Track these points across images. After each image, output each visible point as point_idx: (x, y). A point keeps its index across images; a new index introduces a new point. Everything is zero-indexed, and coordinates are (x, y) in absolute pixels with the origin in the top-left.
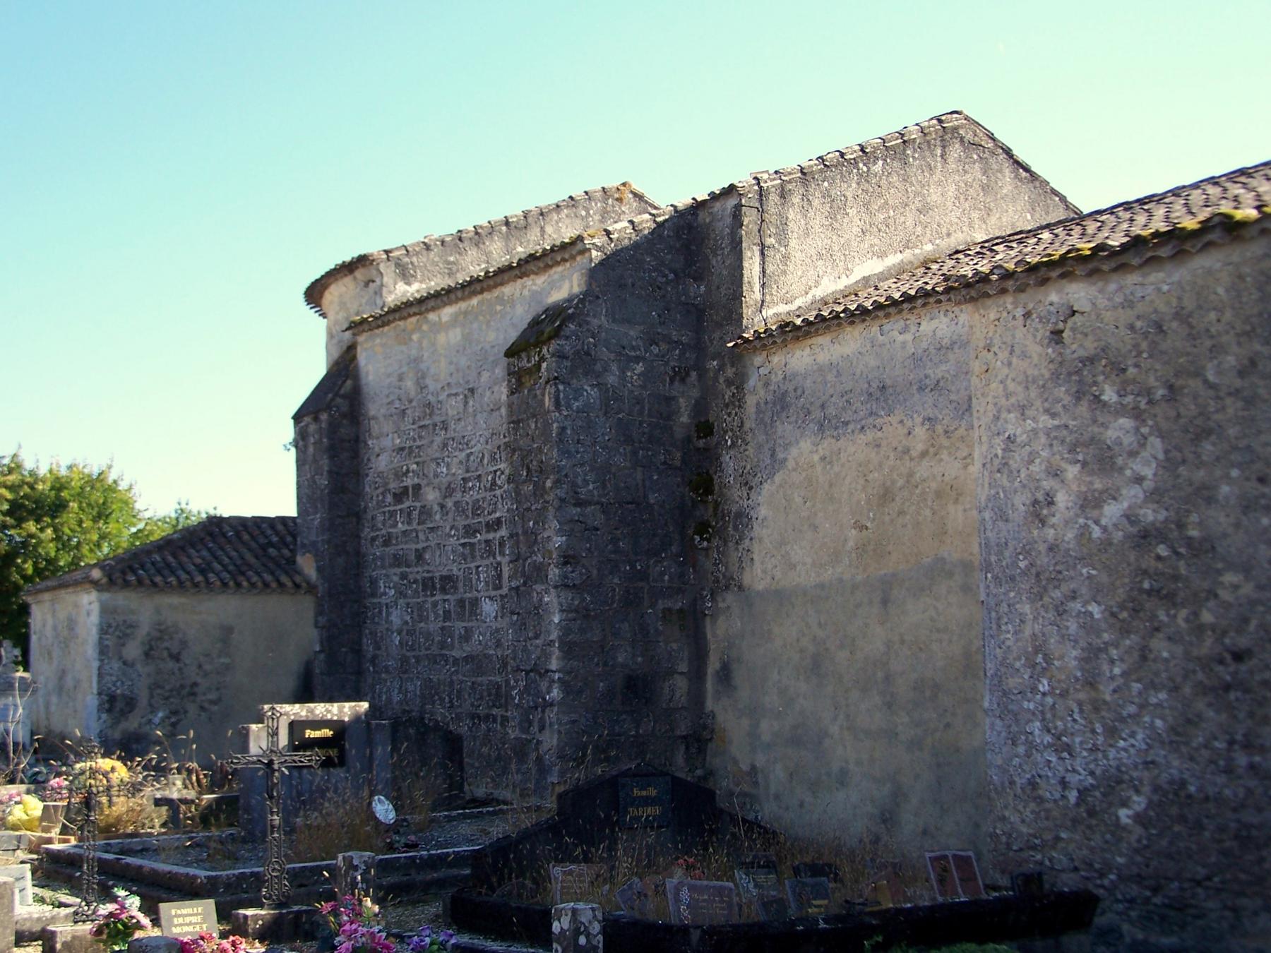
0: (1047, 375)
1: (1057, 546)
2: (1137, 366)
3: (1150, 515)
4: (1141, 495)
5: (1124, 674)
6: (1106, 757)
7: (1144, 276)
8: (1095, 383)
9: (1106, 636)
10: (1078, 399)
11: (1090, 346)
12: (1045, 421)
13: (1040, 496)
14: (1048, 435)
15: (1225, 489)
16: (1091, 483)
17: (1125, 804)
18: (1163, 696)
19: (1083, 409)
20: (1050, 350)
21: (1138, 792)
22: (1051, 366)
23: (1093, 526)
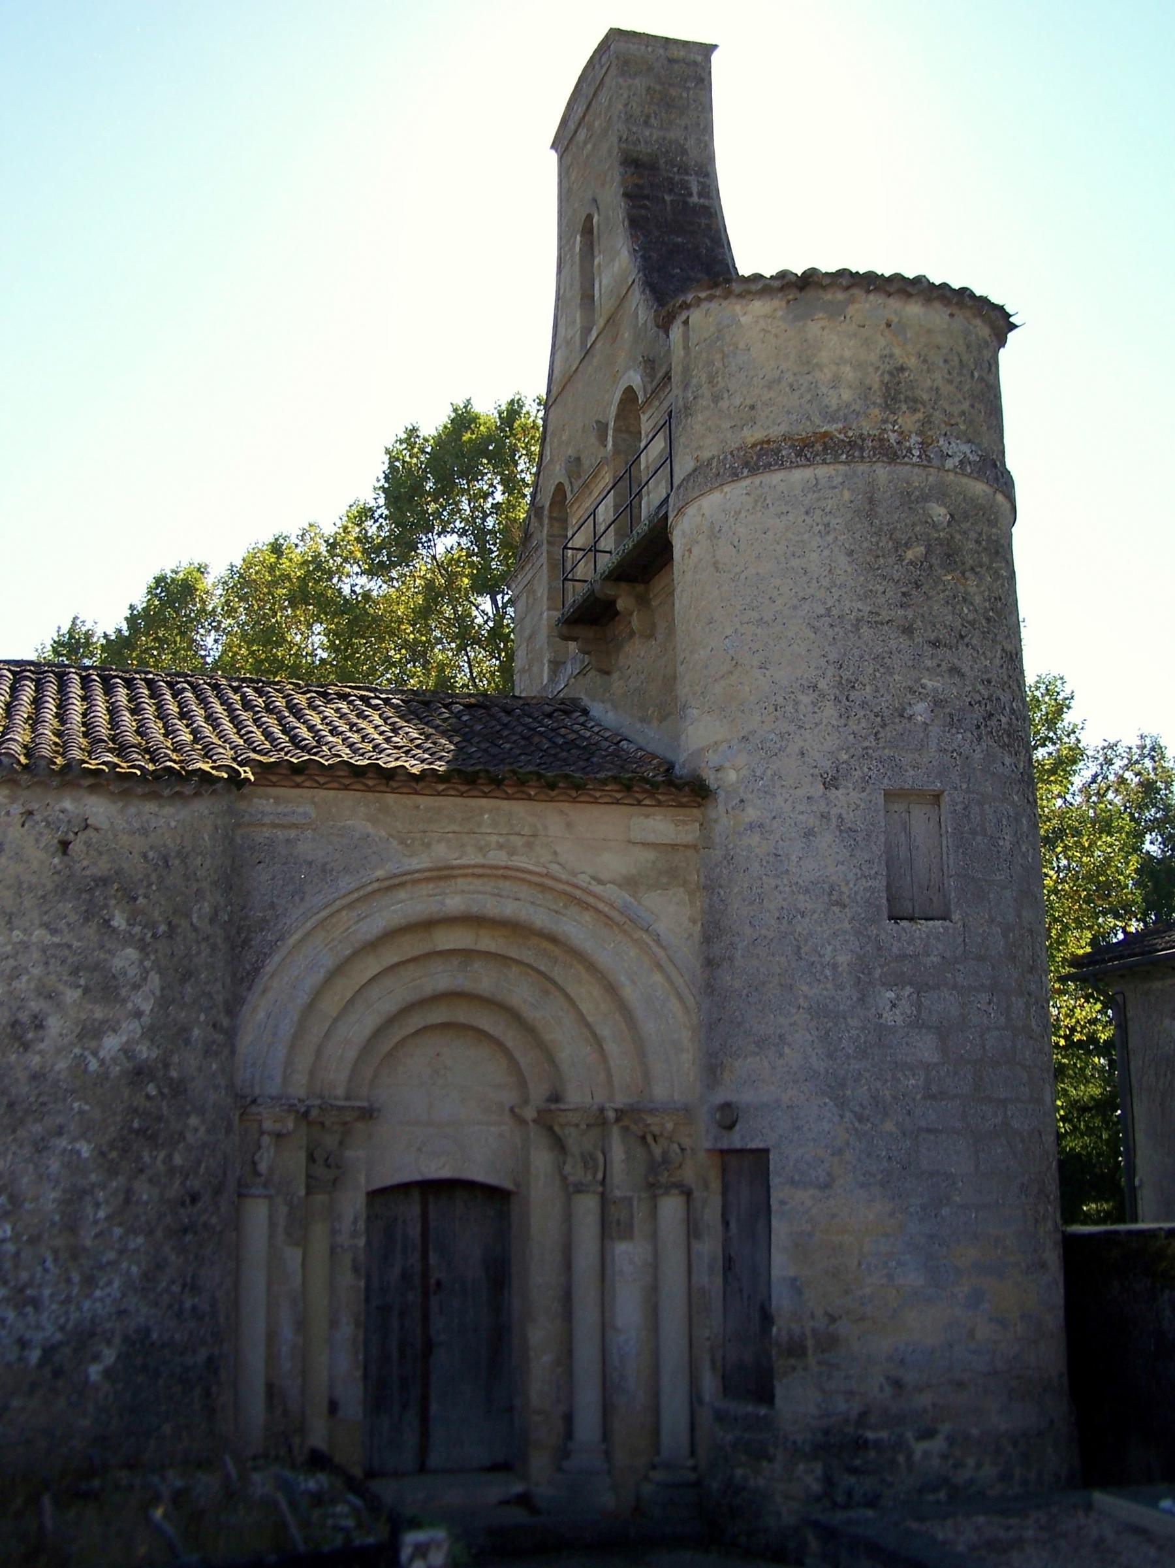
0: (50, 886)
1: (44, 1075)
2: (146, 896)
3: (144, 1052)
4: (139, 1031)
5: (108, 1218)
6: (80, 1309)
7: (161, 806)
8: (106, 906)
9: (93, 1177)
10: (87, 920)
11: (103, 867)
12: (39, 934)
13: (24, 1017)
14: (44, 951)
15: (196, 1032)
16: (91, 1011)
17: (96, 1358)
18: (140, 1240)
19: (90, 931)
20: (56, 860)
21: (109, 1343)
22: (56, 877)
23: (90, 1057)
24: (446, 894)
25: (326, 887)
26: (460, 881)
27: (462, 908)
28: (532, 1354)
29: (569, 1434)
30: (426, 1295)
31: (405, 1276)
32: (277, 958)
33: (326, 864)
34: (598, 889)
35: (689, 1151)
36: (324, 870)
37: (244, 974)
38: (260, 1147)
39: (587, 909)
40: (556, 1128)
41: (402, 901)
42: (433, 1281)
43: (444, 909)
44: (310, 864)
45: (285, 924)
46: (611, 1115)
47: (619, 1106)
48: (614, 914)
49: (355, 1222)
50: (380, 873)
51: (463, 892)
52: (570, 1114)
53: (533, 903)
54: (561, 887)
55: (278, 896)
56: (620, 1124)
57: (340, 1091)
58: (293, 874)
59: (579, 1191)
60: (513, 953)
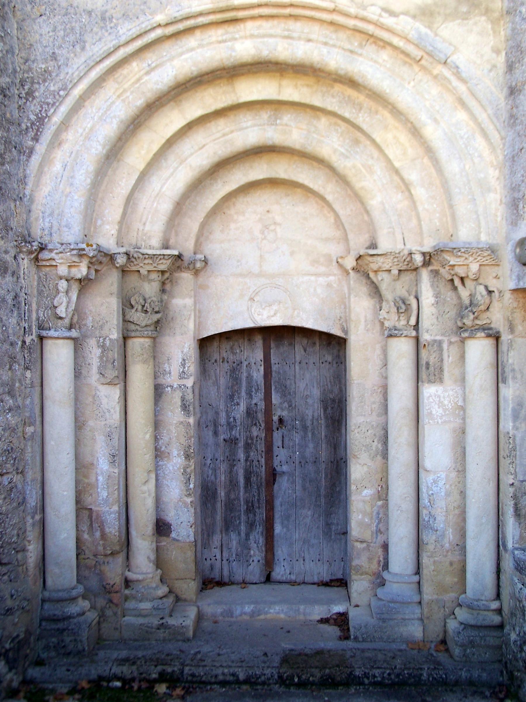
24: (236, 39)
25: (106, 34)
26: (249, 25)
27: (253, 52)
28: (353, 487)
29: (386, 566)
30: (269, 430)
31: (250, 413)
32: (63, 109)
33: (106, 11)
34: (389, 21)
35: (497, 293)
36: (103, 19)
37: (29, 125)
38: (58, 292)
39: (383, 47)
40: (372, 275)
41: (192, 50)
42: (275, 418)
43: (234, 54)
44: (90, 13)
45: (67, 73)
46: (418, 259)
47: (426, 249)
48: (410, 49)
49: (183, 365)
50: (160, 18)
51: (252, 36)
52: (380, 259)
53: (326, 44)
54: (351, 23)
55: (60, 47)
56: (430, 268)
57: (155, 242)
58: (74, 24)
59: (390, 336)
60: (317, 102)
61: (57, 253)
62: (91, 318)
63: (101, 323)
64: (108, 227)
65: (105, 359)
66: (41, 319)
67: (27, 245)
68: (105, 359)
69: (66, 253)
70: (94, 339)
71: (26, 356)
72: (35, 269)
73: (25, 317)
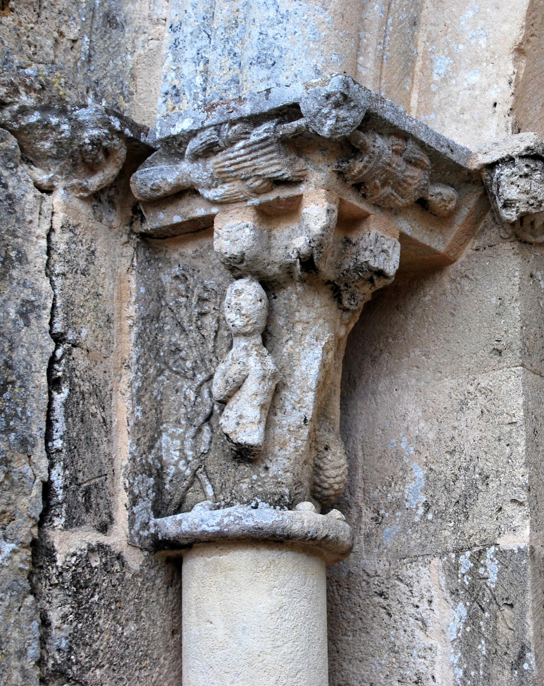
61: (196, 157)
62: (420, 473)
63: (461, 485)
64: (474, 78)
65: (482, 648)
66: (172, 470)
67: (54, 120)
68: (482, 648)
69: (231, 143)
70: (436, 562)
71: (54, 617)
72: (129, 250)
73: (48, 437)
